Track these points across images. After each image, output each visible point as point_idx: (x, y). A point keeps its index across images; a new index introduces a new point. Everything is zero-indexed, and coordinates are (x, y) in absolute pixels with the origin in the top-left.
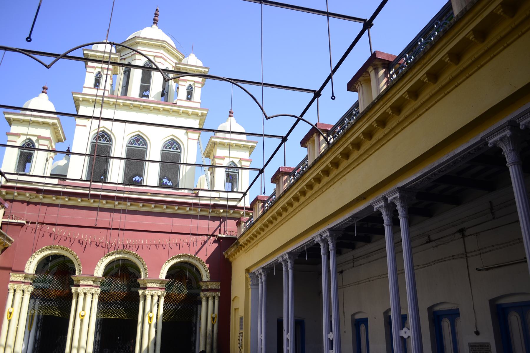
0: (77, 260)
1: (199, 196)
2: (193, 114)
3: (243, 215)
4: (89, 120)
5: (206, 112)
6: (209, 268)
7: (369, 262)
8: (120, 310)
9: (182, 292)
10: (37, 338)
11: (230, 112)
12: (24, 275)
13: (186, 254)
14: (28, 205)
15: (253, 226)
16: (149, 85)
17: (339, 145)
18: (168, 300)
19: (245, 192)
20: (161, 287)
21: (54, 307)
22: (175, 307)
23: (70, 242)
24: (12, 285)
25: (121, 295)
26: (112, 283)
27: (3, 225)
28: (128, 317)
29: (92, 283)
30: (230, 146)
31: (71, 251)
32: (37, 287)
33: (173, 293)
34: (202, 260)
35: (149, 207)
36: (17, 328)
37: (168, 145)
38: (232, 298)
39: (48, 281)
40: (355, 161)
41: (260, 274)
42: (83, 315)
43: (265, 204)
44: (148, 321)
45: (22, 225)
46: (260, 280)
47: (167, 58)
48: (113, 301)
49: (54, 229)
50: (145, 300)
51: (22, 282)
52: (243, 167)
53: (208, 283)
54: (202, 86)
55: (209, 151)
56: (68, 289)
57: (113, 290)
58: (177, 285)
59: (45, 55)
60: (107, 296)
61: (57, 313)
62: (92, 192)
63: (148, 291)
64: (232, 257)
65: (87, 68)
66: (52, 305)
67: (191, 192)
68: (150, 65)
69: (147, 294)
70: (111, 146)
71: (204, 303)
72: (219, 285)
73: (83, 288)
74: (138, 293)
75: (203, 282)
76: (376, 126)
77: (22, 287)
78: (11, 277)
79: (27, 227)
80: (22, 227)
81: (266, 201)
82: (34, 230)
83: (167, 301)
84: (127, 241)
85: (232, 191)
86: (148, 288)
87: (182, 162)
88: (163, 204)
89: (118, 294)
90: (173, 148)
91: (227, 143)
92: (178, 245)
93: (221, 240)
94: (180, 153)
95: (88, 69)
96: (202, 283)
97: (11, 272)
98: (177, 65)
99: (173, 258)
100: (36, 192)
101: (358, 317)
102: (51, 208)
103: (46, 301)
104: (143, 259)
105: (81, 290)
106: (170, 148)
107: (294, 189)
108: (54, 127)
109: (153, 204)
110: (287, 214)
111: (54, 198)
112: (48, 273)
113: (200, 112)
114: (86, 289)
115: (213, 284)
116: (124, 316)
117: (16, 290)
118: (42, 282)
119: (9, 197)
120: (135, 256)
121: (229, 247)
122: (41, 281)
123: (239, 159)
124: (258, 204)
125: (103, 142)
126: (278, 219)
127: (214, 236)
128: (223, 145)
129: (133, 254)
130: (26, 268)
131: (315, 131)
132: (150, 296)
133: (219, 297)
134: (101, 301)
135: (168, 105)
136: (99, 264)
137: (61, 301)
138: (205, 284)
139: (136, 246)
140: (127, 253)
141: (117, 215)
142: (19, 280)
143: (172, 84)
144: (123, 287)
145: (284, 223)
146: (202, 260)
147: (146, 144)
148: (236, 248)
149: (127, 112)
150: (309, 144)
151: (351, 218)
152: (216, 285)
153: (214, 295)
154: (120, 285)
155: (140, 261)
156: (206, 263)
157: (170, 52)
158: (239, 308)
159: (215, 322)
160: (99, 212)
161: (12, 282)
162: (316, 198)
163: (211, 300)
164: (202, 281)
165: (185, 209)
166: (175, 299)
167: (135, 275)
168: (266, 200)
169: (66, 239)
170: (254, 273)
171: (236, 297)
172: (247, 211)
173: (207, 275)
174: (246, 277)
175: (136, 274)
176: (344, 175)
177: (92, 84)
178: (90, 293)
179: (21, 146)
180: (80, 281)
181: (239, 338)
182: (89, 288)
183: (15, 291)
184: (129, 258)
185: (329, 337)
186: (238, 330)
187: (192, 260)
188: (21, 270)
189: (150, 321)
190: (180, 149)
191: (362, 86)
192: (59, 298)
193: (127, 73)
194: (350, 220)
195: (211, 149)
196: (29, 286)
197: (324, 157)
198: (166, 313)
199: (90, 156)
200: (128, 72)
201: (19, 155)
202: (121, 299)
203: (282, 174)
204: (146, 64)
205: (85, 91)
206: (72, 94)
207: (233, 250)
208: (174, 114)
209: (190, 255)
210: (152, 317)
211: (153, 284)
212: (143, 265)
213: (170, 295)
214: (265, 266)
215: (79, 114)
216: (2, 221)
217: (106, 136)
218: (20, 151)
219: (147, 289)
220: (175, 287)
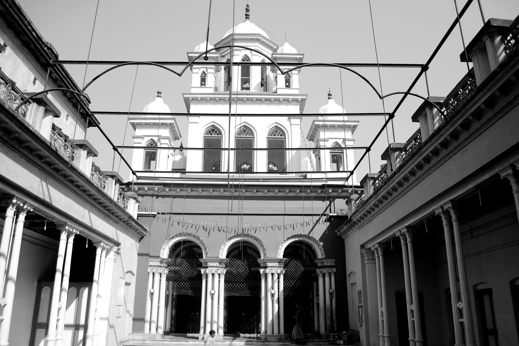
0: (203, 244)
1: (308, 178)
2: (293, 100)
3: (351, 193)
4: (199, 117)
5: (306, 97)
6: (323, 246)
7: (490, 232)
8: (244, 288)
9: (299, 270)
10: (173, 315)
11: (329, 95)
12: (160, 260)
13: (300, 234)
14: (157, 198)
15: (367, 203)
16: (249, 78)
17: (458, 117)
18: (287, 278)
19: (352, 170)
20: (279, 266)
21: (187, 287)
22: (294, 284)
23: (196, 228)
24: (151, 269)
25: (244, 274)
26: (235, 264)
27: (138, 217)
28: (251, 295)
29: (218, 265)
30: (333, 128)
31: (198, 237)
32: (171, 270)
33: (290, 271)
34: (315, 239)
35: (263, 192)
36: (158, 306)
37: (273, 133)
38: (348, 274)
39: (179, 265)
40: (476, 131)
41: (376, 249)
43: (375, 181)
44: (271, 297)
45: (154, 216)
46: (376, 255)
47: (263, 50)
48: (237, 280)
49: (181, 217)
50: (266, 278)
51: (159, 266)
52: (347, 147)
53: (323, 260)
54: (299, 73)
55: (312, 135)
56: (196, 271)
57: (236, 270)
58: (294, 262)
59: (171, 64)
60: (231, 276)
61: (190, 293)
62: (231, 183)
63: (268, 270)
64: (345, 234)
65: (193, 70)
66: (185, 286)
67: (300, 174)
68: (247, 59)
69: (267, 272)
70: (222, 139)
71: (321, 280)
72: (334, 262)
73: (211, 270)
74: (259, 272)
75: (319, 259)
76: (498, 95)
77: (159, 271)
78: (149, 262)
79: (158, 218)
80: (154, 218)
81: (377, 178)
82: (164, 220)
83: (285, 279)
84: (245, 225)
85: (338, 171)
86: (268, 267)
87: (287, 147)
88: (275, 189)
89: (241, 274)
90: (278, 135)
91: (329, 125)
92: (292, 226)
93: (332, 219)
94: (285, 139)
95: (194, 71)
96: (317, 260)
97: (149, 257)
98: (274, 56)
99: (288, 239)
100: (163, 186)
101: (479, 288)
102: (176, 199)
103: (180, 282)
104: (261, 240)
105: (209, 271)
106: (275, 135)
107: (411, 164)
108: (172, 126)
109: (266, 189)
110: (403, 189)
111: (178, 190)
112: (178, 256)
113: (300, 97)
114: (214, 270)
115: (328, 261)
116: (248, 293)
117: (155, 273)
118: (175, 266)
119: (141, 192)
121: (341, 225)
122: (173, 265)
123: (343, 140)
124: (368, 182)
125: (214, 135)
126: (393, 195)
127: (325, 215)
128: (325, 127)
129: (252, 237)
130: (161, 254)
131: (427, 105)
132: (271, 275)
133: (335, 273)
134: (227, 280)
135: (269, 95)
136: (222, 247)
137: (192, 282)
139: (254, 229)
140: (246, 236)
141: (236, 202)
142: (156, 264)
143: (270, 74)
145: (400, 198)
146: (315, 239)
147: (252, 133)
148: (349, 225)
149: (251, 106)
150: (421, 118)
151: (474, 188)
152: (331, 262)
153: (330, 271)
156: (320, 242)
157: (264, 44)
158: (356, 283)
159: (333, 297)
160: (233, 200)
161: (151, 266)
162: (434, 171)
163: (327, 277)
164: (317, 258)
165: (295, 192)
166: (293, 276)
167: (253, 256)
168: (376, 177)
169: (192, 226)
170: (370, 248)
171: (352, 272)
172: (356, 189)
173: (322, 253)
174: (361, 252)
175: (254, 255)
176: (465, 146)
177: (199, 85)
178: (218, 274)
179: (146, 146)
181: (359, 311)
182: (216, 269)
183: (154, 274)
184: (248, 241)
185: (458, 305)
186: (357, 304)
187: (306, 239)
188: (157, 255)
189: (273, 298)
190: (285, 135)
191: (477, 56)
192: (190, 279)
193: (227, 69)
194: (474, 190)
195: (314, 133)
196: (165, 270)
197: (442, 130)
198: (286, 290)
199: (205, 150)
200: (228, 69)
201: (145, 155)
202: (244, 278)
203: (393, 150)
204: (244, 59)
205: (193, 91)
206: (183, 95)
207: (345, 227)
208: (275, 102)
211: (272, 263)
212: (262, 246)
213: (288, 273)
214: (381, 241)
215: (191, 113)
216: (138, 214)
217: (216, 130)
218: (145, 151)
219: (267, 268)
220: (292, 266)
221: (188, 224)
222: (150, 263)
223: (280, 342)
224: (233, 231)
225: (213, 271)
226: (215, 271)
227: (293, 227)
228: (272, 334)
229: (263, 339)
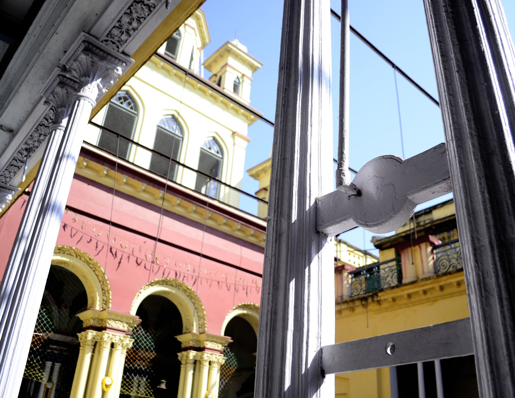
0: (100, 282)
23: (97, 247)
29: (125, 327)
42: (108, 383)
73: (113, 335)
88: (238, 222)
92: (245, 288)
105: (109, 337)
114: (117, 337)
129: (186, 290)
132: (207, 364)
139: (192, 277)
140: (176, 287)
144: (150, 343)
154: (146, 338)
155: (194, 303)
169: (91, 240)
180: (108, 320)
190: (222, 154)
219: (204, 350)
224: (161, 272)
226: (120, 339)
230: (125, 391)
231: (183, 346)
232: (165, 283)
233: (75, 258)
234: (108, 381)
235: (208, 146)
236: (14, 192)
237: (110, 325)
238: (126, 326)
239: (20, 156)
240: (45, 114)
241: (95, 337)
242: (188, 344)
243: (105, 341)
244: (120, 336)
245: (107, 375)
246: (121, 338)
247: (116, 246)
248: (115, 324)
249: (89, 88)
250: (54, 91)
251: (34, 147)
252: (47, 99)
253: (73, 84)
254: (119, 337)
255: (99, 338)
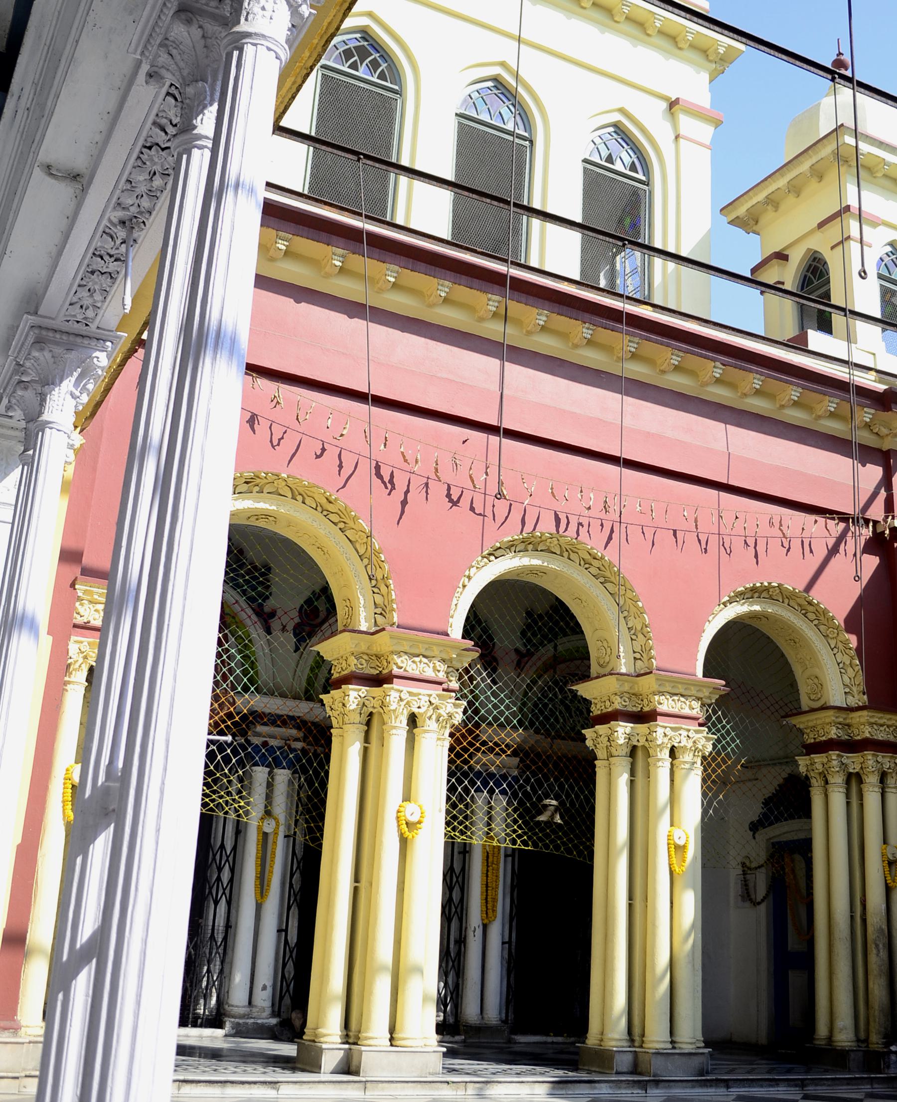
23: (341, 466)
34: (833, 618)
42: (414, 819)
78: (77, 604)
92: (751, 542)
105: (401, 700)
111: (282, 245)
115: (881, 721)
116: (519, 836)
120: (593, 570)
129: (588, 562)
138: (841, 720)
139: (602, 525)
146: (833, 618)
152: (888, 726)
154: (494, 694)
169: (323, 450)
187: (789, 614)
190: (647, 171)
209: (794, 589)
210: (684, 847)
221: (299, 436)
222: (81, 609)
223: (711, 1086)
225: (422, 703)
227: (755, 547)
228: (670, 1046)
229: (625, 1070)
230: (457, 834)
231: (596, 711)
232: (530, 547)
233: (289, 499)
234: (411, 812)
235: (605, 153)
236: (109, 344)
237: (401, 668)
238: (443, 667)
239: (109, 244)
240: (154, 112)
241: (367, 703)
242: (608, 703)
243: (394, 711)
244: (430, 696)
245: (407, 798)
246: (433, 701)
247: (390, 459)
248: (414, 666)
249: (263, 8)
250: (167, 39)
251: (141, 213)
252: (152, 66)
253: (217, 8)
254: (427, 699)
255: (377, 704)
